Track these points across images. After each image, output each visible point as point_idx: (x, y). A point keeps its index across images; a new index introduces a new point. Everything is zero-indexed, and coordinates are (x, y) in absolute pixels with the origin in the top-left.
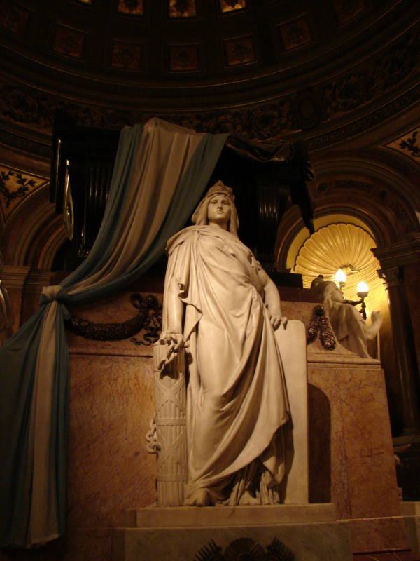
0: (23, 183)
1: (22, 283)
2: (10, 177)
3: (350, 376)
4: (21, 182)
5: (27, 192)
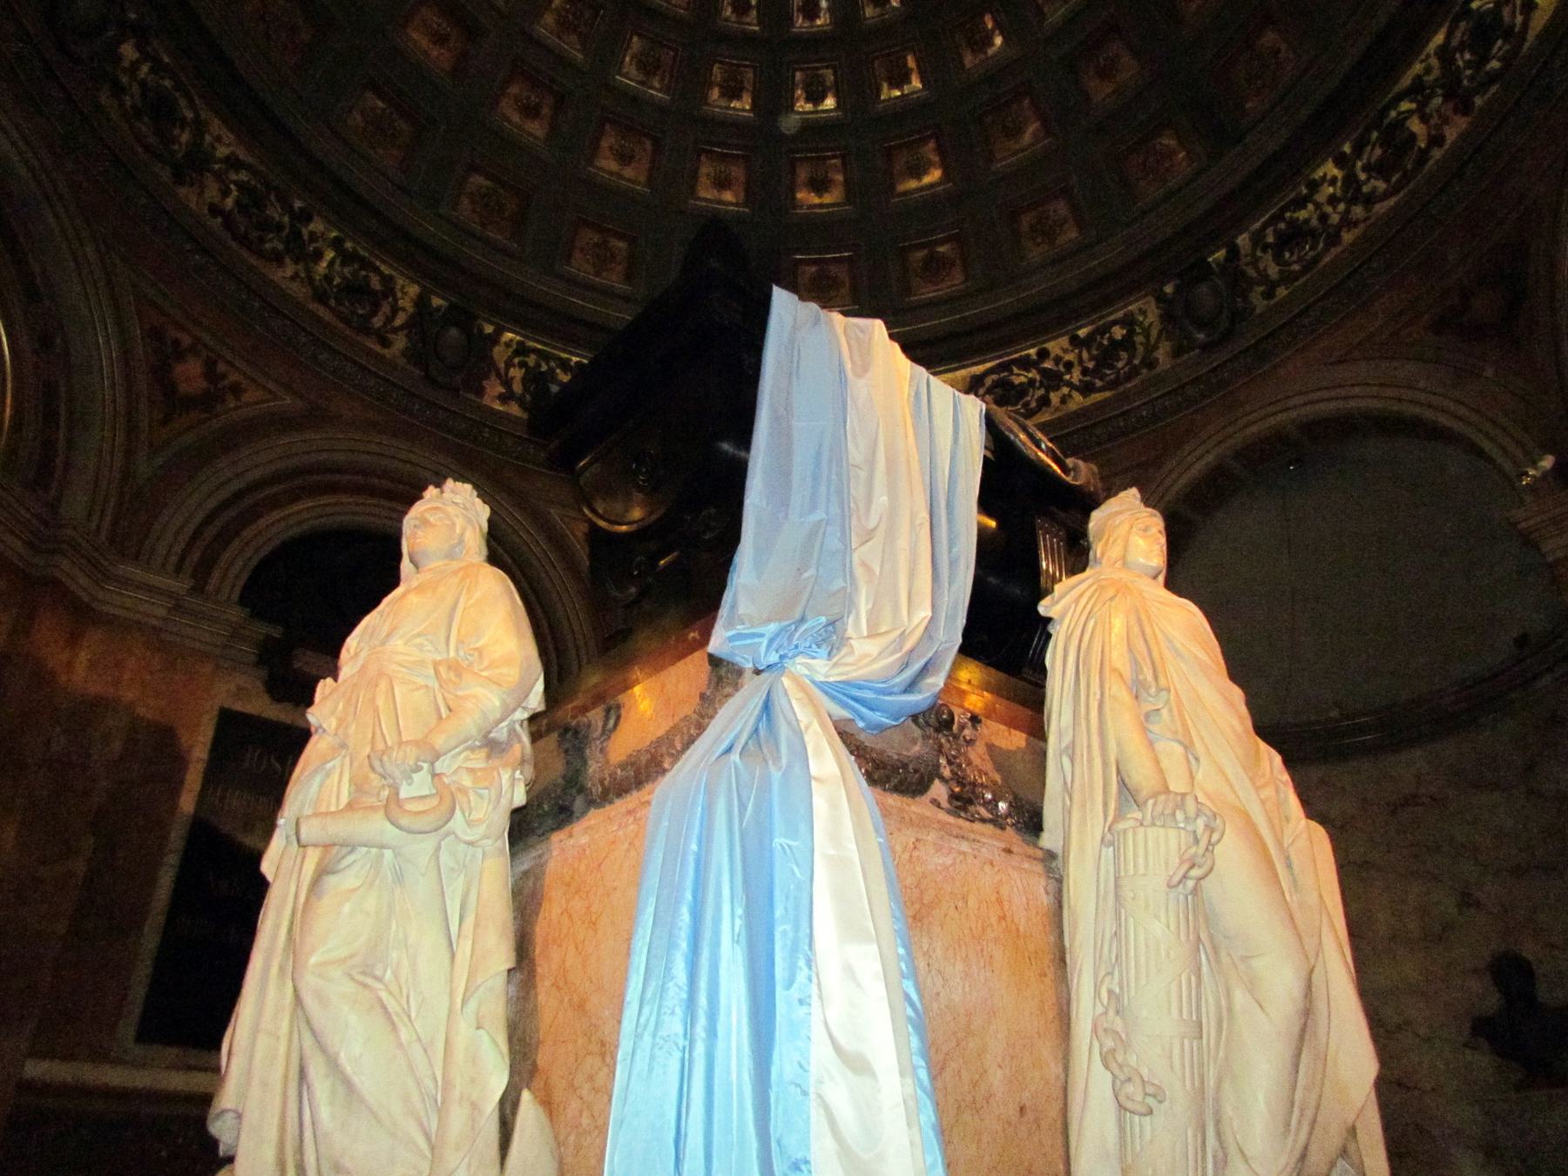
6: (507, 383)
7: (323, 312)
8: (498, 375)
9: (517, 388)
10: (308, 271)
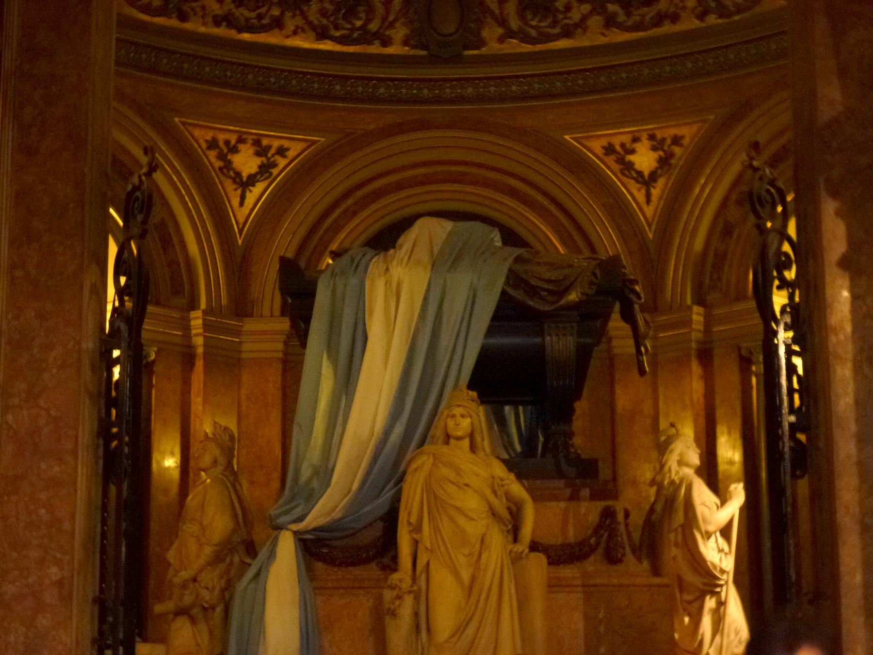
0: (266, 156)
1: (280, 346)
2: (241, 147)
3: (627, 602)
4: (261, 151)
5: (275, 171)
6: (503, 22)
7: (327, 46)
8: (496, 19)
9: (514, 23)
10: (305, 17)
